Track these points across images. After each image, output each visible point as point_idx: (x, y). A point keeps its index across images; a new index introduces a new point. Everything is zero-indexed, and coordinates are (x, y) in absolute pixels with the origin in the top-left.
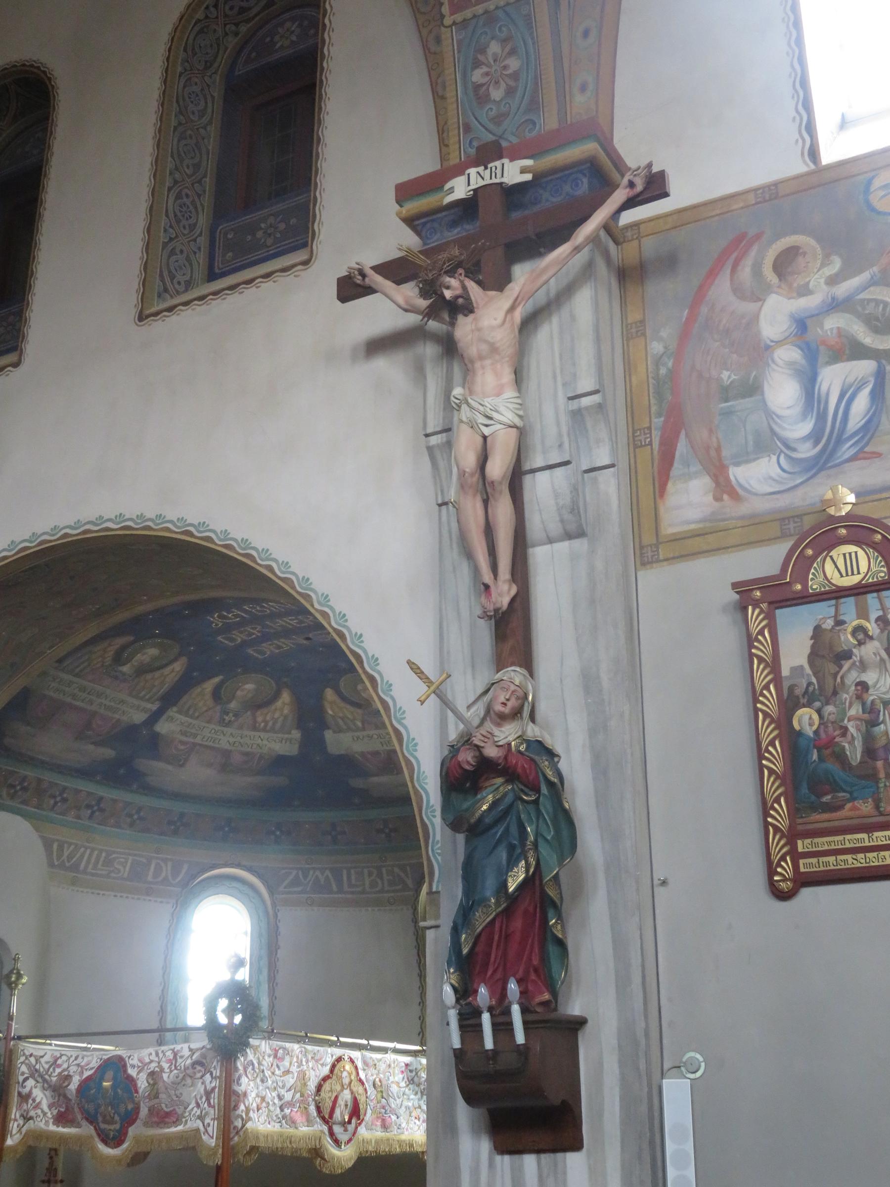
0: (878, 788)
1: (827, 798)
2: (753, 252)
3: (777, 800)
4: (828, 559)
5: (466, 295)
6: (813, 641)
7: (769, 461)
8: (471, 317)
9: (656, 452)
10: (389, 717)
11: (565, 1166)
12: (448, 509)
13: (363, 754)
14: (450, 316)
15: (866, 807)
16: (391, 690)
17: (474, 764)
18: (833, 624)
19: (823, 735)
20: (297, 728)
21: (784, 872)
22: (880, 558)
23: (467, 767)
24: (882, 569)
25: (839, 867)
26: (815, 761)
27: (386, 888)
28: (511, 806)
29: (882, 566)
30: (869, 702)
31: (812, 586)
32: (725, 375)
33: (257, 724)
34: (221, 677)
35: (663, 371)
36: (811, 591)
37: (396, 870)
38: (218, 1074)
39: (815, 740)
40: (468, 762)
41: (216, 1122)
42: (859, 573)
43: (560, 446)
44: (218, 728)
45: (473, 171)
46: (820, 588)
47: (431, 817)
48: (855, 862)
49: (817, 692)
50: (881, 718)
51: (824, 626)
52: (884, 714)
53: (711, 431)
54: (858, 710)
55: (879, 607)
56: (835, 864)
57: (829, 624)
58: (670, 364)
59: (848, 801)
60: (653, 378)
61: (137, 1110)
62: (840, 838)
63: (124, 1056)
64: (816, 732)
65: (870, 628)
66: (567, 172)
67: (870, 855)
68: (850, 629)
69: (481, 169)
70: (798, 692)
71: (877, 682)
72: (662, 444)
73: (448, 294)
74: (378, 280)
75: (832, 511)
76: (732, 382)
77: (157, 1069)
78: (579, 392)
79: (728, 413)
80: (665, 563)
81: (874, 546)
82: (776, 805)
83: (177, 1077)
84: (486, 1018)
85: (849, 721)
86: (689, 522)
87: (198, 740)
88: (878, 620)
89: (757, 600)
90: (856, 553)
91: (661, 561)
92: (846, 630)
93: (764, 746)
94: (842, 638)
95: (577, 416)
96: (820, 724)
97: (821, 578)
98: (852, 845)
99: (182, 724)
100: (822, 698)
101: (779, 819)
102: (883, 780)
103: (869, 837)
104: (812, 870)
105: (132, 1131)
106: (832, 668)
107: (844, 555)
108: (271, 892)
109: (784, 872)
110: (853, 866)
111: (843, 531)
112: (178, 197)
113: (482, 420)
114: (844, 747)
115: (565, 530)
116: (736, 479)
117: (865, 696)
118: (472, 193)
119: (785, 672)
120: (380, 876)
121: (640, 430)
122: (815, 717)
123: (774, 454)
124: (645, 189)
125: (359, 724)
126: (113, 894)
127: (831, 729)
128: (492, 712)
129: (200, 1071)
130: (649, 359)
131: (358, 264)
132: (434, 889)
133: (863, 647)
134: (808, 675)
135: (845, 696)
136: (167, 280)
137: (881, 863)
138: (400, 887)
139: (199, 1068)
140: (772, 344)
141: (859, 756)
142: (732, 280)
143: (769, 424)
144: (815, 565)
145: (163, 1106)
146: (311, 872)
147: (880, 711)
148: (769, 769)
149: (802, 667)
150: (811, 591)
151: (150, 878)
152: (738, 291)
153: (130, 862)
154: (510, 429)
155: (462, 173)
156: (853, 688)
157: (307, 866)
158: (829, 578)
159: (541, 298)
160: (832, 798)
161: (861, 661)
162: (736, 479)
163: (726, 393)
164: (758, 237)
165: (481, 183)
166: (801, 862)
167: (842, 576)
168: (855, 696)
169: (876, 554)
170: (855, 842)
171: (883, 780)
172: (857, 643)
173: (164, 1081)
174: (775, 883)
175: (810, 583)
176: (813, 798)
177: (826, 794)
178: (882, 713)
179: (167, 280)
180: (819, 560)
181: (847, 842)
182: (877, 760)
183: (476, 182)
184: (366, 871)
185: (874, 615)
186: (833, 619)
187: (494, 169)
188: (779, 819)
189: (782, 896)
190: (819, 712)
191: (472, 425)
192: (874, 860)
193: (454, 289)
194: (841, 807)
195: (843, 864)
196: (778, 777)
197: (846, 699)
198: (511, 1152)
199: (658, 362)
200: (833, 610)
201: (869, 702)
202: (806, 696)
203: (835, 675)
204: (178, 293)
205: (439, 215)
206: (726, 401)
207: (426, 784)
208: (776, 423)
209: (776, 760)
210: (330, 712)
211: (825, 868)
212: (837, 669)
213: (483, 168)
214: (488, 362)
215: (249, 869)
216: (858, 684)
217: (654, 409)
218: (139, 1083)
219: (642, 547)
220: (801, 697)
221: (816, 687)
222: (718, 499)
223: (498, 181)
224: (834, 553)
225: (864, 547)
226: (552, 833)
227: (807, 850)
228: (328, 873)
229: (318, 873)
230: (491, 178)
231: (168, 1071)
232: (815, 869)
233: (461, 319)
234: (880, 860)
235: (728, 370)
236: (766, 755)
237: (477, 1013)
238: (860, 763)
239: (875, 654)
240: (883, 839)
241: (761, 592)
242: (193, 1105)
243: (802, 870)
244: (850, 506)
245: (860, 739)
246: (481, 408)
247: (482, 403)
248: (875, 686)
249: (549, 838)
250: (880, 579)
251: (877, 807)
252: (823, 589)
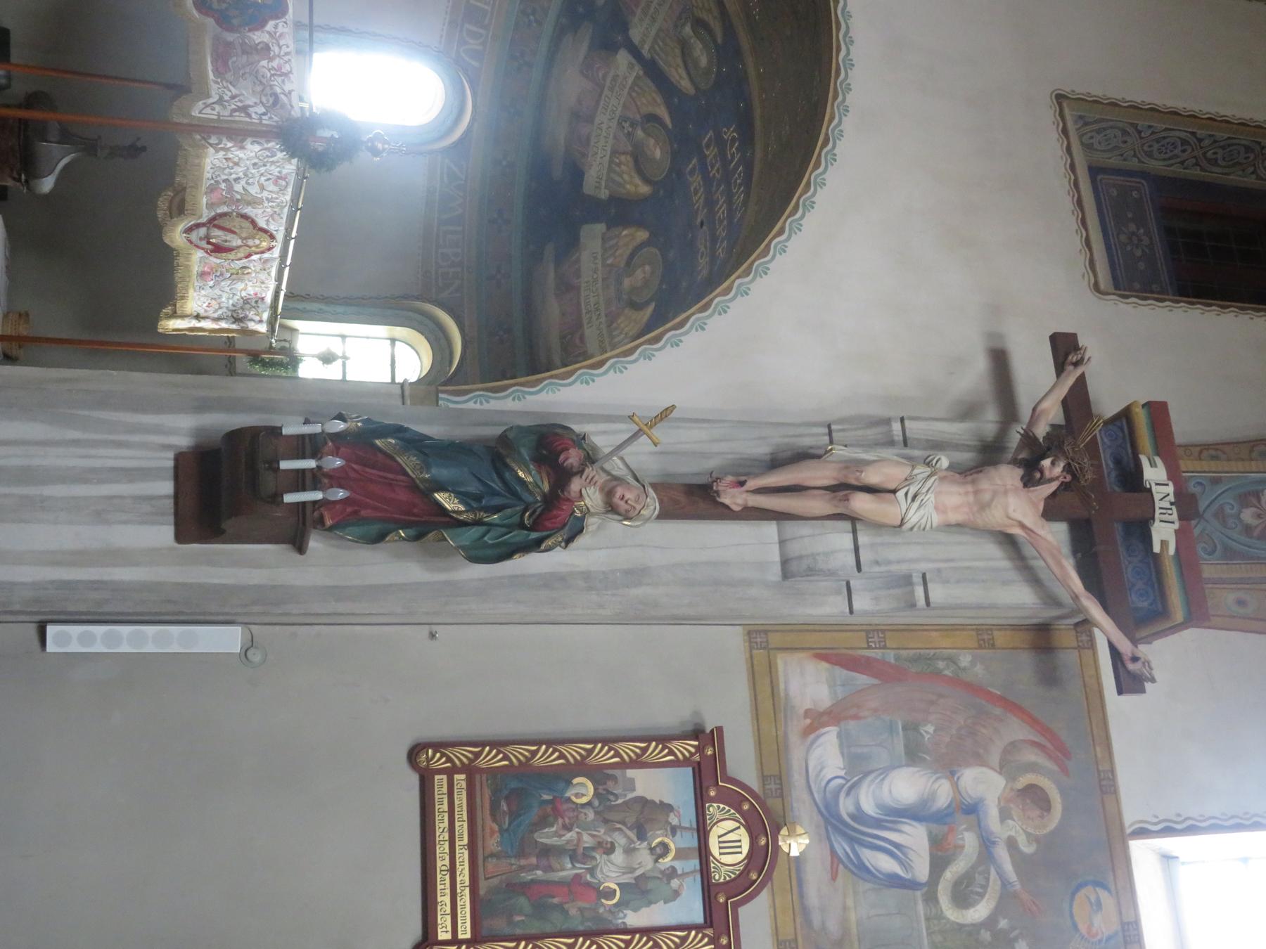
0: (510, 857)
1: (504, 806)
2: (1048, 764)
3: (506, 758)
4: (738, 825)
5: (1042, 481)
6: (658, 802)
7: (840, 768)
8: (1020, 484)
9: (860, 652)
10: (617, 356)
11: (162, 524)
12: (824, 435)
13: (578, 261)
14: (1023, 459)
15: (493, 845)
16: (645, 359)
17: (565, 465)
18: (673, 824)
19: (565, 806)
20: (610, 195)
21: (435, 760)
22: (733, 876)
23: (562, 457)
24: (723, 878)
25: (437, 814)
26: (541, 796)
28: (520, 499)
29: (725, 878)
30: (594, 854)
31: (711, 806)
32: (930, 729)
33: (617, 155)
34: (670, 126)
35: (941, 665)
36: (707, 805)
38: (264, 122)
39: (562, 797)
40: (567, 459)
41: (215, 117)
42: (721, 854)
43: (877, 563)
44: (618, 113)
45: (1170, 489)
47: (513, 396)
48: (441, 830)
49: (608, 803)
50: (578, 865)
51: (672, 815)
52: (581, 868)
53: (875, 710)
54: (586, 842)
55: (686, 871)
56: (440, 810)
57: (674, 820)
58: (947, 672)
59: (500, 826)
60: (934, 655)
61: (231, 29)
62: (465, 818)
63: (287, 17)
64: (569, 800)
65: (666, 860)
66: (1156, 585)
67: (446, 845)
68: (667, 840)
69: (1172, 498)
70: (610, 784)
71: (613, 864)
72: (868, 660)
73: (1046, 463)
74: (1069, 381)
75: (784, 831)
76: (921, 734)
77: (272, 53)
78: (930, 585)
79: (891, 729)
80: (748, 655)
81: (745, 872)
82: (501, 756)
83: (263, 76)
84: (311, 464)
85: (578, 833)
86: (786, 683)
87: (606, 92)
88: (673, 869)
89: (703, 751)
90: (741, 853)
91: (751, 651)
92: (666, 836)
93: (560, 748)
94: (659, 832)
95: (907, 580)
96: (577, 804)
97: (718, 816)
98: (457, 828)
99: (625, 78)
100: (601, 808)
101: (488, 758)
102: (518, 863)
103: (464, 846)
104: (436, 787)
105: (210, 22)
106: (631, 820)
107: (740, 841)
109: (435, 760)
110: (437, 828)
111: (763, 842)
112: (1184, 142)
113: (913, 490)
114: (553, 826)
115: (792, 559)
116: (825, 733)
117: (600, 850)
118: (1148, 486)
119: (630, 773)
121: (884, 637)
122: (584, 800)
123: (846, 773)
124: (1129, 672)
125: (609, 262)
127: (571, 814)
128: (615, 483)
129: (268, 101)
130: (955, 651)
131: (1089, 359)
132: (441, 395)
133: (648, 852)
134: (625, 796)
135: (603, 831)
136: (1095, 127)
137: (438, 855)
139: (271, 100)
140: (955, 779)
141: (541, 840)
142: (1024, 741)
143: (877, 770)
144: (732, 811)
145: (234, 59)
147: (584, 864)
148: (536, 752)
149: (633, 790)
150: (707, 805)
151: (467, 26)
152: (1012, 747)
153: (486, 7)
154: (900, 519)
155: (1170, 478)
156: (609, 840)
158: (718, 824)
159: (1028, 551)
160: (504, 811)
161: (634, 849)
162: (825, 733)
163: (911, 728)
164: (1065, 771)
165: (1157, 497)
166: (445, 777)
167: (719, 837)
168: (601, 840)
169: (737, 872)
170: (460, 831)
171: (518, 863)
172: (653, 846)
173: (259, 61)
174: (425, 750)
175: (715, 805)
176: (506, 792)
177: (508, 805)
178: (582, 866)
179: (1095, 127)
180: (737, 815)
181: (461, 823)
182: (537, 858)
183: (1158, 492)
185: (679, 865)
186: (678, 824)
187: (1170, 512)
188: (488, 758)
189: (414, 754)
190: (589, 804)
191: (908, 480)
192: (442, 849)
193: (1051, 469)
194: (494, 820)
195: (440, 818)
196: (528, 759)
197: (599, 832)
198: (176, 468)
199: (952, 660)
200: (687, 825)
201: (594, 854)
202: (605, 792)
203: (624, 823)
204: (1081, 137)
205: (1129, 445)
206: (905, 728)
207: (547, 392)
208: (876, 778)
209: (544, 760)
210: (625, 232)
211: (436, 800)
212: (629, 825)
213: (1173, 500)
214: (971, 498)
216: (612, 844)
217: (904, 653)
218: (258, 33)
219: (766, 632)
220: (605, 787)
221: (613, 803)
222: (807, 713)
223: (1157, 515)
224: (742, 830)
226: (490, 542)
227: (455, 783)
230: (1161, 508)
231: (270, 67)
232: (436, 790)
233: (1019, 472)
234: (441, 855)
235: (935, 731)
236: (551, 750)
237: (315, 454)
238: (536, 842)
239: (639, 864)
240: (461, 860)
241: (710, 755)
242: (234, 91)
243: (437, 777)
244: (786, 850)
245: (559, 843)
246: (924, 490)
247: (930, 492)
248: (609, 862)
249: (486, 538)
250: (713, 875)
251: (492, 855)
252: (708, 817)
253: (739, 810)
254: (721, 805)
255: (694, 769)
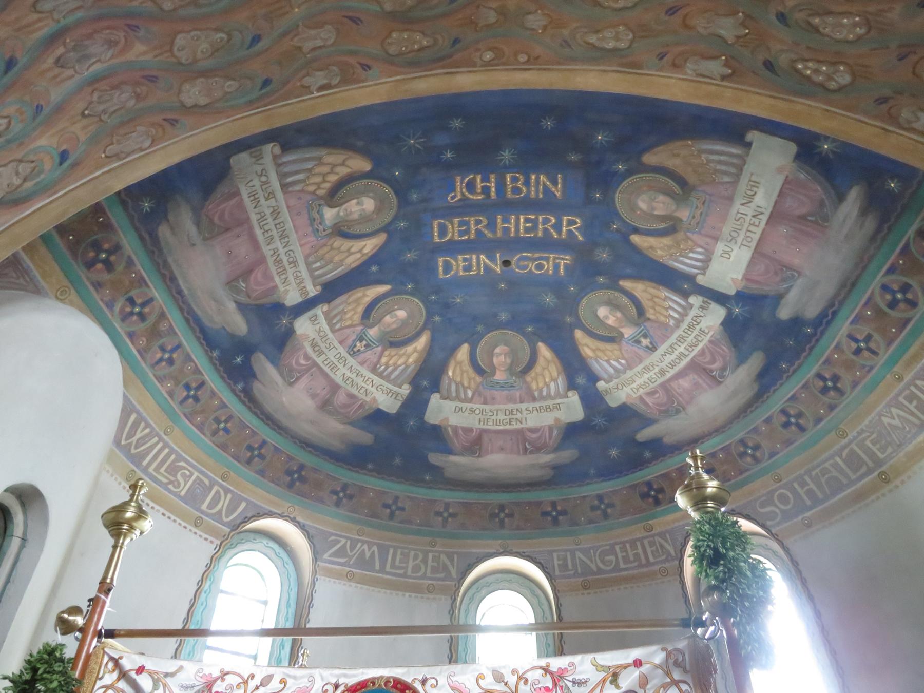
13: (455, 429)
20: (410, 383)
27: (429, 574)
33: (378, 366)
37: (443, 558)
44: (344, 354)
63: (409, 680)
87: (319, 361)
99: (320, 331)
108: (316, 556)
120: (425, 561)
125: (470, 393)
126: (162, 510)
138: (442, 575)
146: (359, 545)
151: (204, 507)
153: (193, 478)
157: (357, 537)
184: (412, 553)
210: (450, 373)
215: (302, 527)
228: (375, 548)
229: (366, 547)
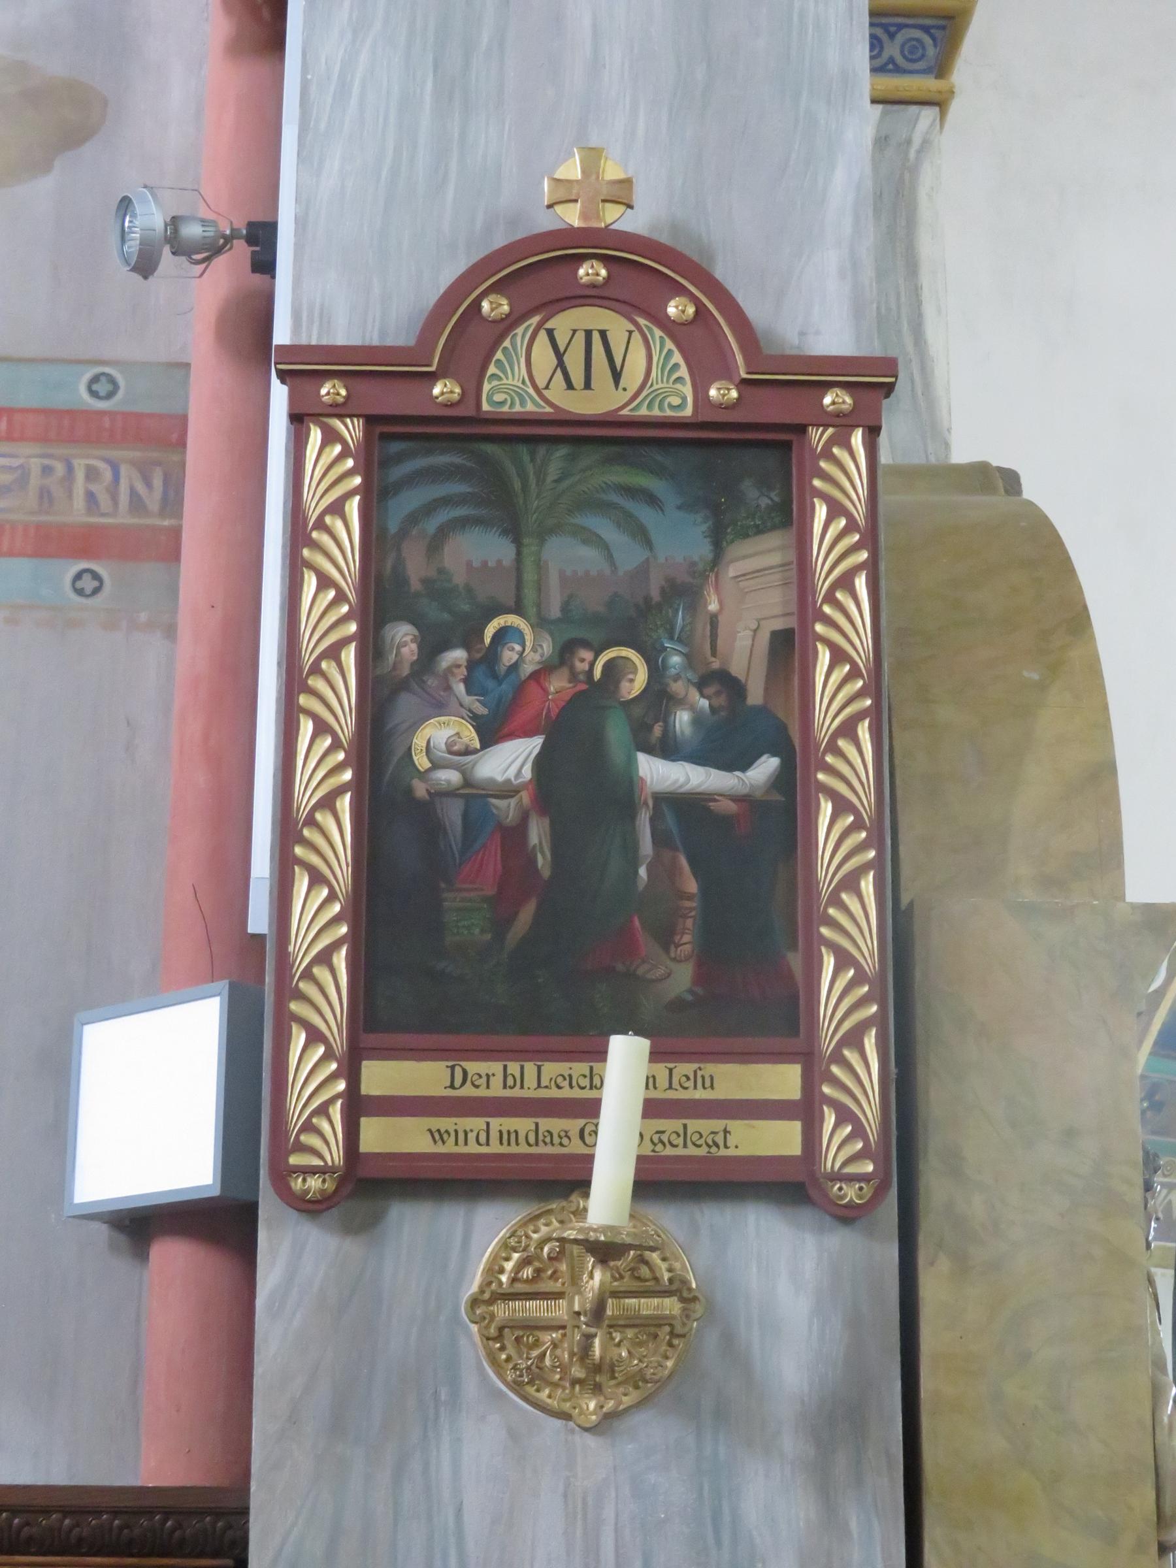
24: (678, 386)
46: (512, 404)
144: (507, 343)
150: (485, 407)
175: (486, 387)
225: (642, 321)
252: (518, 408)
253: (508, 325)
254: (489, 373)
255: (384, 437)
